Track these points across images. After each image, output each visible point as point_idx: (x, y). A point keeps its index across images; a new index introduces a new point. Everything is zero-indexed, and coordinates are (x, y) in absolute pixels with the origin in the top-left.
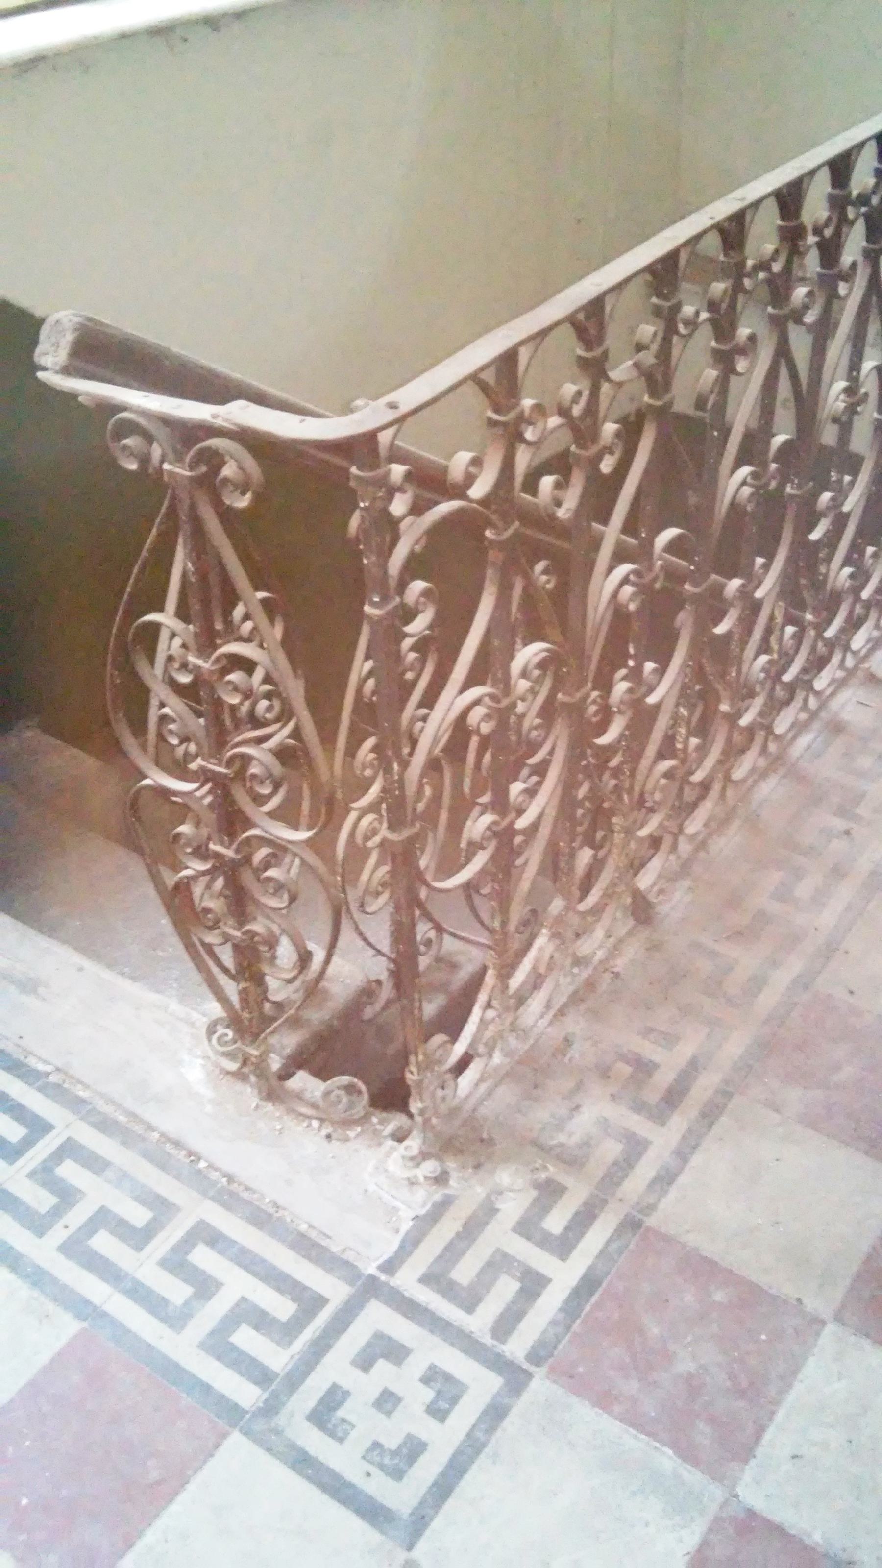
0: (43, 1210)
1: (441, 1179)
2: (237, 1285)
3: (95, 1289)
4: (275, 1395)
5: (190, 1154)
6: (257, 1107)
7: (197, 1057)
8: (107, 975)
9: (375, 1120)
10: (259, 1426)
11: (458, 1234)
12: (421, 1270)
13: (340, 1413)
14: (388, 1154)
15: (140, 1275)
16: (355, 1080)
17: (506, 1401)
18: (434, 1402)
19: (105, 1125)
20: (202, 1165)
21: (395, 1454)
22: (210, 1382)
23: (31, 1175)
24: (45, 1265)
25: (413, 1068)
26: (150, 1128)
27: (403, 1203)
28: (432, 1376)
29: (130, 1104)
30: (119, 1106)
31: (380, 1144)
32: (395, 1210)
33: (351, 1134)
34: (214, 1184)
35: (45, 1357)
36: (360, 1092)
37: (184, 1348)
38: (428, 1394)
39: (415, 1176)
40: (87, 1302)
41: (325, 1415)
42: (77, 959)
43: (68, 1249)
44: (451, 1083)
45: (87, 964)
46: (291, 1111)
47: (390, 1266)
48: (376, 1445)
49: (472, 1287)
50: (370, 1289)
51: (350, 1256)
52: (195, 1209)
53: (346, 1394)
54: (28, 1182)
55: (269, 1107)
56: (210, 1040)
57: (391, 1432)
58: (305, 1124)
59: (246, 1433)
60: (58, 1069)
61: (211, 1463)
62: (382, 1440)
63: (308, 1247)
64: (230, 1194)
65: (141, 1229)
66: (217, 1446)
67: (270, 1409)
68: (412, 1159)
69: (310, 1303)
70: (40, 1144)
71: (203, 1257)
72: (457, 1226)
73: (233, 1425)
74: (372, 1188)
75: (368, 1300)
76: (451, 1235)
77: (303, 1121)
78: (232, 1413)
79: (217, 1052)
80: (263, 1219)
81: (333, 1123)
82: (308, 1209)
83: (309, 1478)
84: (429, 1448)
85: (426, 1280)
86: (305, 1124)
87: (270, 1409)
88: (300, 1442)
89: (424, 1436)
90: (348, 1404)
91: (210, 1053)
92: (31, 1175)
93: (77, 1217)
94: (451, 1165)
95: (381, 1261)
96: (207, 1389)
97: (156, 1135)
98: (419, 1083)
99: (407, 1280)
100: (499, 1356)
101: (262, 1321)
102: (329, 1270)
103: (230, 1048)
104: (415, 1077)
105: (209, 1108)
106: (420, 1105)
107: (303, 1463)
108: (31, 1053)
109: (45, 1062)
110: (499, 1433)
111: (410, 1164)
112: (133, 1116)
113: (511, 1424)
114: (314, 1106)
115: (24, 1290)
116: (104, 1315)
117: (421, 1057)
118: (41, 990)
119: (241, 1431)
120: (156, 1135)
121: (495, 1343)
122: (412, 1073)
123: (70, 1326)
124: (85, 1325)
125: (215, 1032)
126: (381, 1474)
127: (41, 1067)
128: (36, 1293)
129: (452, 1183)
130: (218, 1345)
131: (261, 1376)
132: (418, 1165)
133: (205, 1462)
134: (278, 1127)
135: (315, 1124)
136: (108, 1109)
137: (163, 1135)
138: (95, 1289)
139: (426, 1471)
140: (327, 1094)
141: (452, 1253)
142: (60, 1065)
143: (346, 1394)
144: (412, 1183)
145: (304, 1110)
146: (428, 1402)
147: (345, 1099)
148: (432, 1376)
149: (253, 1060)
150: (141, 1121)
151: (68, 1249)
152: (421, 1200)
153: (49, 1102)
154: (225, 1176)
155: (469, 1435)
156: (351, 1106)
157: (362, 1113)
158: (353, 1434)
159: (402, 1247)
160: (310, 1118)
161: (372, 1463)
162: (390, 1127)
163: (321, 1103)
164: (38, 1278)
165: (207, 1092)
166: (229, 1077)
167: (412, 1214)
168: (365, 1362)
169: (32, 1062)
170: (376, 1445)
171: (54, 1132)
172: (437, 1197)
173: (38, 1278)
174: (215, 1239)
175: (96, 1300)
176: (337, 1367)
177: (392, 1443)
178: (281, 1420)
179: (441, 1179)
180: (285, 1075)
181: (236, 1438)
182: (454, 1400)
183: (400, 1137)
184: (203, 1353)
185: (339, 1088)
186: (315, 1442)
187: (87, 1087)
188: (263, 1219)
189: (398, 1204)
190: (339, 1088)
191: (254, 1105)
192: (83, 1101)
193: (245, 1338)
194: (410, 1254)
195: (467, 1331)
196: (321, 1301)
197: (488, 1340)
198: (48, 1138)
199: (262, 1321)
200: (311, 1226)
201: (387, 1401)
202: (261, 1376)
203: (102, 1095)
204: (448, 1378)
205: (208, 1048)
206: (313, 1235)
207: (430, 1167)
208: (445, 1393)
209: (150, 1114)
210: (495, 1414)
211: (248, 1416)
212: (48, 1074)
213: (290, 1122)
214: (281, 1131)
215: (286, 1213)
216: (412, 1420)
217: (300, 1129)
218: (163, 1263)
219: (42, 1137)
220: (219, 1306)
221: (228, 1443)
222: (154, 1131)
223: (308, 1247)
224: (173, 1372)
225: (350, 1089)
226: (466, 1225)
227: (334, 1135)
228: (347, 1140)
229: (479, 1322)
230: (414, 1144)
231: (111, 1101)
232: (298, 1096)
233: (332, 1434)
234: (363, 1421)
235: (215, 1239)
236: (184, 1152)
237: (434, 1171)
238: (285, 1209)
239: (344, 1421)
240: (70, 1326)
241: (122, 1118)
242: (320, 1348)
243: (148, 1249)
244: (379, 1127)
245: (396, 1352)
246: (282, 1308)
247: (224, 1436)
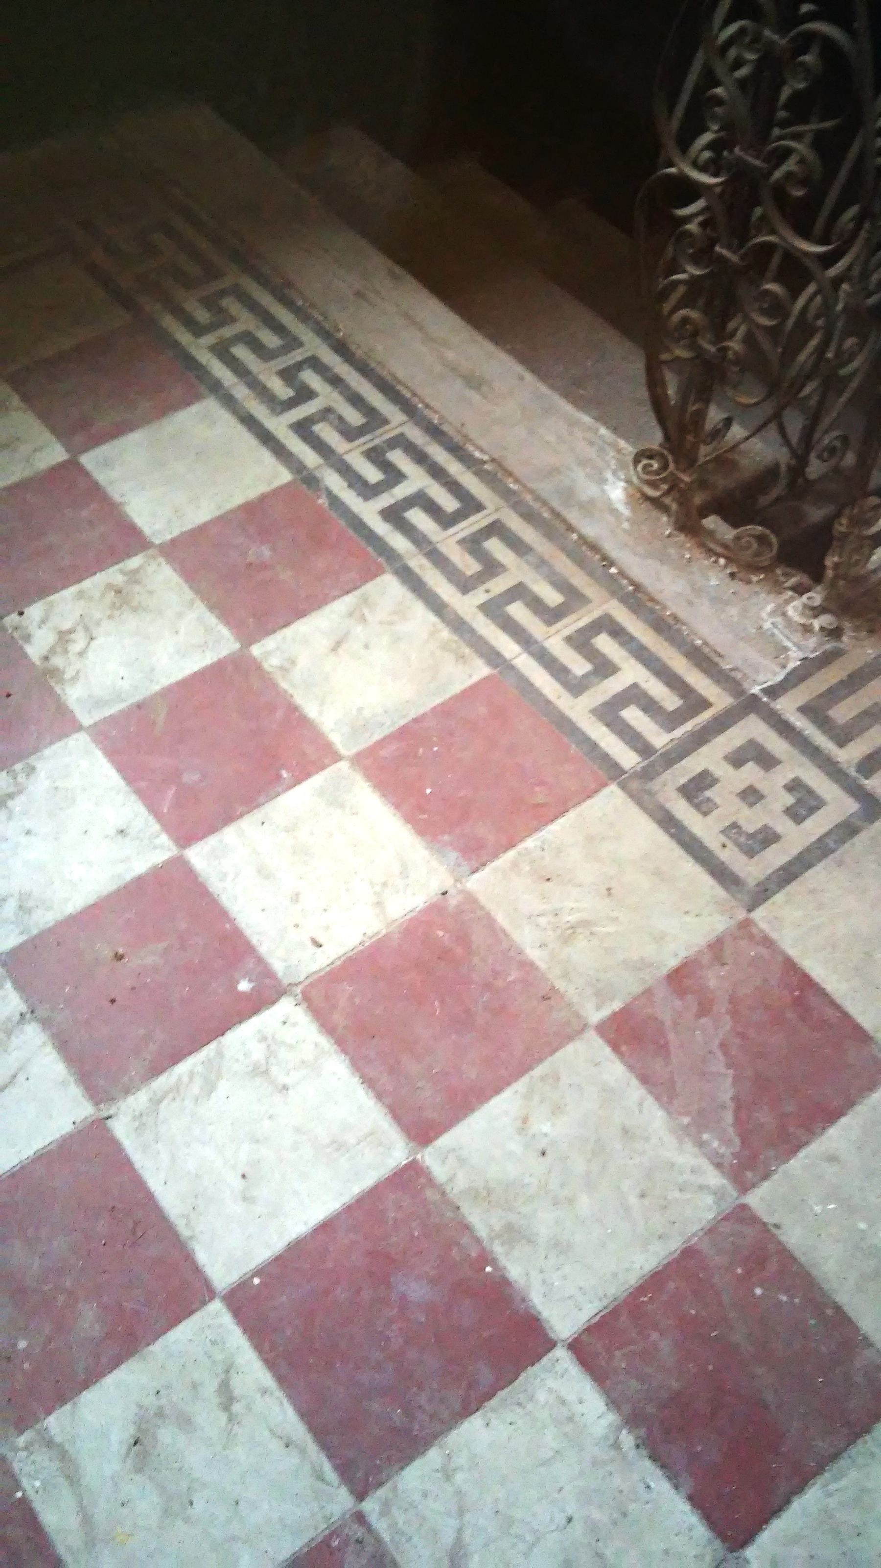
0: (469, 573)
1: (835, 633)
2: (631, 673)
3: (508, 647)
4: (651, 765)
5: (604, 558)
6: (669, 536)
7: (621, 480)
8: (544, 389)
9: (779, 571)
10: (635, 785)
11: (842, 682)
12: (801, 702)
13: (708, 793)
14: (787, 602)
15: (547, 644)
16: (768, 532)
17: (859, 823)
18: (793, 806)
19: (529, 517)
20: (613, 570)
21: (751, 836)
22: (598, 742)
23: (461, 542)
24: (467, 618)
25: (844, 521)
26: (571, 528)
27: (795, 644)
28: (795, 786)
29: (556, 504)
30: (545, 503)
31: (780, 593)
32: (786, 649)
33: (755, 579)
34: (622, 588)
35: (457, 688)
36: (770, 545)
37: (579, 710)
38: (789, 800)
39: (811, 625)
40: (498, 654)
41: (696, 789)
42: (519, 369)
43: (486, 608)
44: (866, 550)
45: (529, 377)
46: (702, 545)
47: (773, 692)
48: (735, 825)
49: (844, 727)
50: (749, 705)
51: (738, 676)
52: (604, 605)
53: (715, 781)
54: (457, 548)
55: (682, 537)
56: (635, 467)
57: (752, 819)
58: (713, 559)
59: (623, 787)
60: (493, 460)
61: (589, 802)
62: (741, 822)
63: (703, 659)
64: (638, 598)
65: (553, 609)
66: (596, 792)
67: (647, 774)
68: (813, 608)
69: (695, 704)
70: (472, 519)
71: (604, 643)
72: (842, 675)
73: (613, 779)
74: (767, 625)
75: (747, 714)
76: (834, 681)
77: (711, 557)
78: (613, 771)
79: (639, 478)
80: (665, 626)
81: (739, 566)
82: (707, 625)
83: (672, 836)
84: (782, 840)
85: (804, 710)
86: (713, 559)
87: (647, 774)
88: (668, 805)
89: (779, 829)
90: (716, 788)
91: (635, 480)
92: (461, 542)
93: (499, 585)
94: (847, 625)
95: (765, 685)
96: (594, 746)
97: (575, 536)
98: (846, 535)
99: (787, 706)
100: (861, 787)
101: (650, 706)
102: (718, 682)
103: (654, 478)
104: (842, 529)
105: (626, 525)
106: (836, 559)
107: (668, 823)
108: (470, 440)
109: (482, 451)
110: (847, 846)
111: (810, 613)
112: (557, 515)
113: (860, 841)
114: (725, 546)
115: (445, 633)
116: (512, 668)
117: (856, 511)
118: (484, 388)
119: (619, 784)
120: (575, 536)
121: (858, 775)
122: (841, 525)
123: (481, 670)
124: (495, 672)
125: (640, 462)
126: (736, 849)
127: (477, 454)
128: (455, 638)
129: (845, 639)
130: (609, 713)
131: (643, 748)
132: (816, 617)
133: (584, 800)
134: (688, 556)
135: (722, 561)
136: (536, 505)
137: (581, 537)
138: (508, 647)
139: (775, 857)
140: (738, 538)
141: (833, 695)
142: (496, 456)
143: (715, 781)
144: (807, 629)
145: (712, 546)
146: (788, 805)
147: (755, 546)
148: (795, 786)
149: (682, 485)
150: (564, 521)
151: (486, 608)
152: (813, 646)
153: (483, 486)
154: (632, 585)
155: (820, 840)
156: (757, 554)
157: (766, 563)
158: (715, 812)
159: (786, 679)
160: (719, 555)
161: (730, 838)
162: (793, 581)
163: (732, 545)
164: (459, 626)
165: (625, 511)
166: (648, 503)
167: (801, 655)
168: (737, 760)
169: (470, 448)
170: (735, 825)
171: (485, 512)
172: (828, 647)
173: (459, 626)
174: (617, 632)
175: (507, 655)
176: (709, 758)
177: (750, 828)
178: (655, 785)
179: (835, 633)
180: (703, 512)
181: (613, 788)
182: (812, 810)
183: (800, 590)
184: (594, 719)
185: (750, 535)
186: (682, 810)
187: (517, 481)
188: (665, 626)
189: (788, 644)
190: (750, 535)
191: (667, 532)
192: (514, 493)
193: (633, 715)
194: (795, 685)
195: (835, 760)
196: (705, 704)
197: (852, 772)
198: (479, 516)
199: (650, 706)
200: (705, 643)
201: (751, 795)
202: (643, 748)
203: (532, 492)
204: (810, 792)
205: (632, 472)
206: (706, 650)
207: (826, 620)
208: (804, 803)
209: (573, 516)
210: (847, 830)
211: (627, 775)
212: (485, 462)
213: (698, 554)
214: (689, 560)
215: (684, 628)
216: (772, 813)
217: (706, 562)
218: (569, 640)
219: (474, 514)
220: (614, 685)
221: (606, 791)
222: (573, 532)
223: (703, 659)
224: (565, 725)
225: (761, 539)
226: (850, 676)
227: (738, 575)
228: (749, 582)
229: (849, 755)
230: (816, 597)
231: (538, 498)
232: (711, 534)
233: (697, 807)
234: (727, 805)
235: (617, 632)
236: (598, 557)
237: (831, 624)
238: (684, 624)
239: (709, 800)
240: (481, 670)
241: (546, 515)
242: (701, 738)
243: (559, 625)
244: (782, 579)
245: (767, 761)
246: (671, 701)
247: (605, 785)
